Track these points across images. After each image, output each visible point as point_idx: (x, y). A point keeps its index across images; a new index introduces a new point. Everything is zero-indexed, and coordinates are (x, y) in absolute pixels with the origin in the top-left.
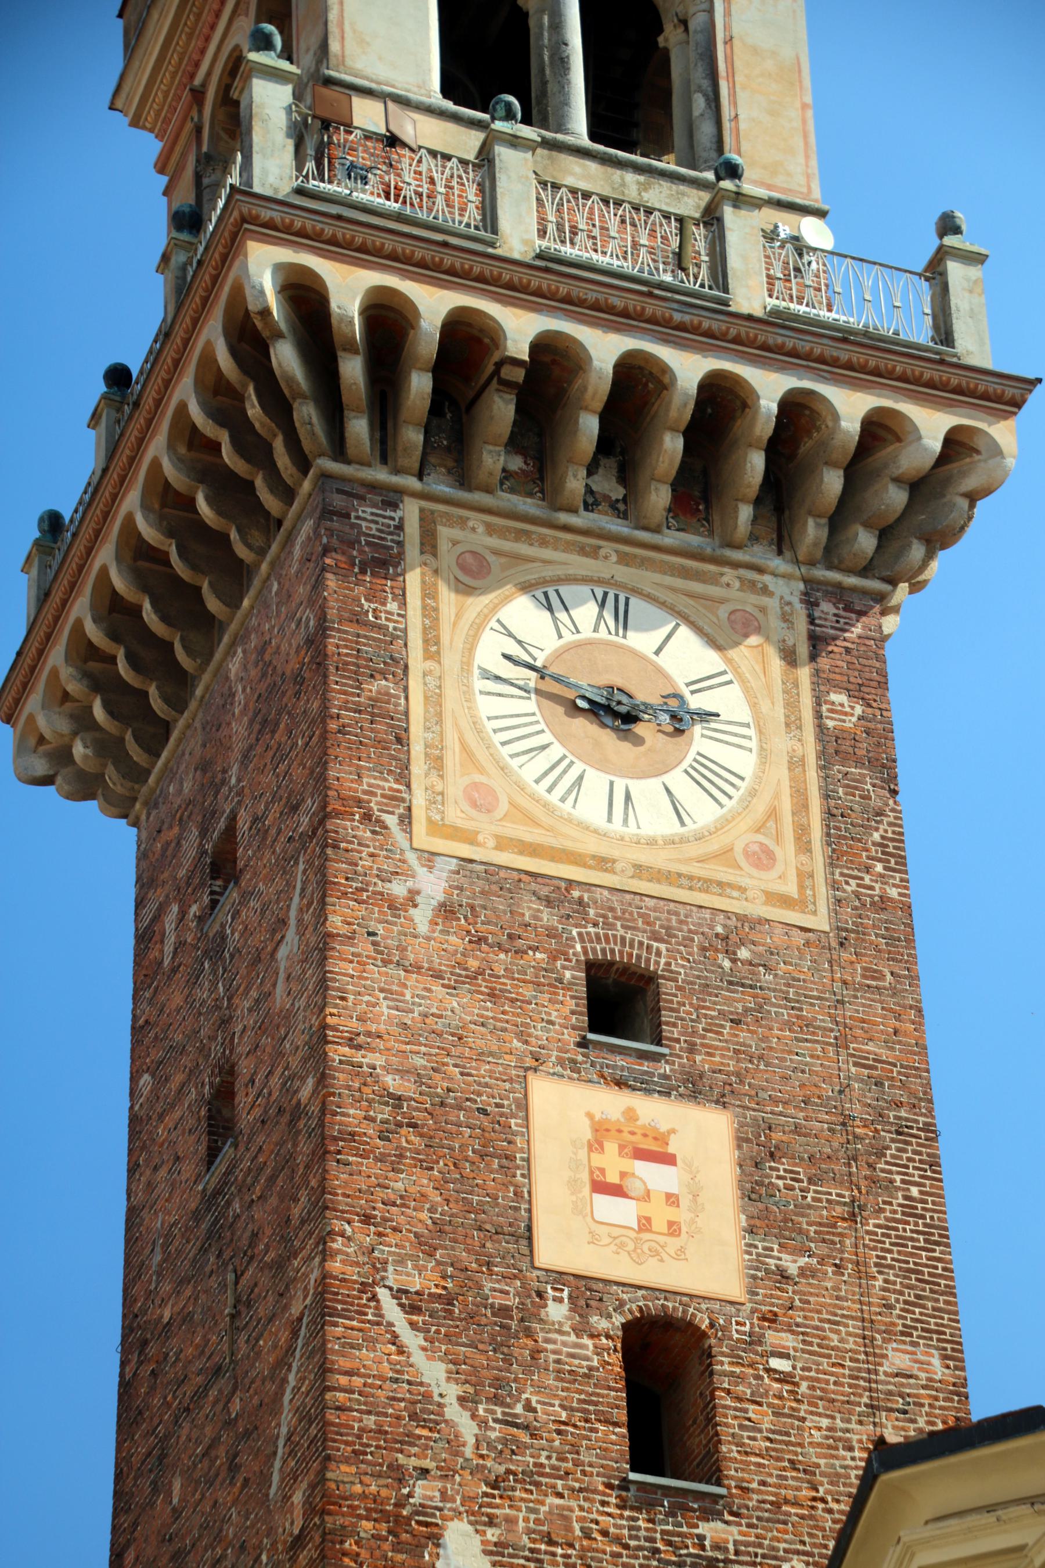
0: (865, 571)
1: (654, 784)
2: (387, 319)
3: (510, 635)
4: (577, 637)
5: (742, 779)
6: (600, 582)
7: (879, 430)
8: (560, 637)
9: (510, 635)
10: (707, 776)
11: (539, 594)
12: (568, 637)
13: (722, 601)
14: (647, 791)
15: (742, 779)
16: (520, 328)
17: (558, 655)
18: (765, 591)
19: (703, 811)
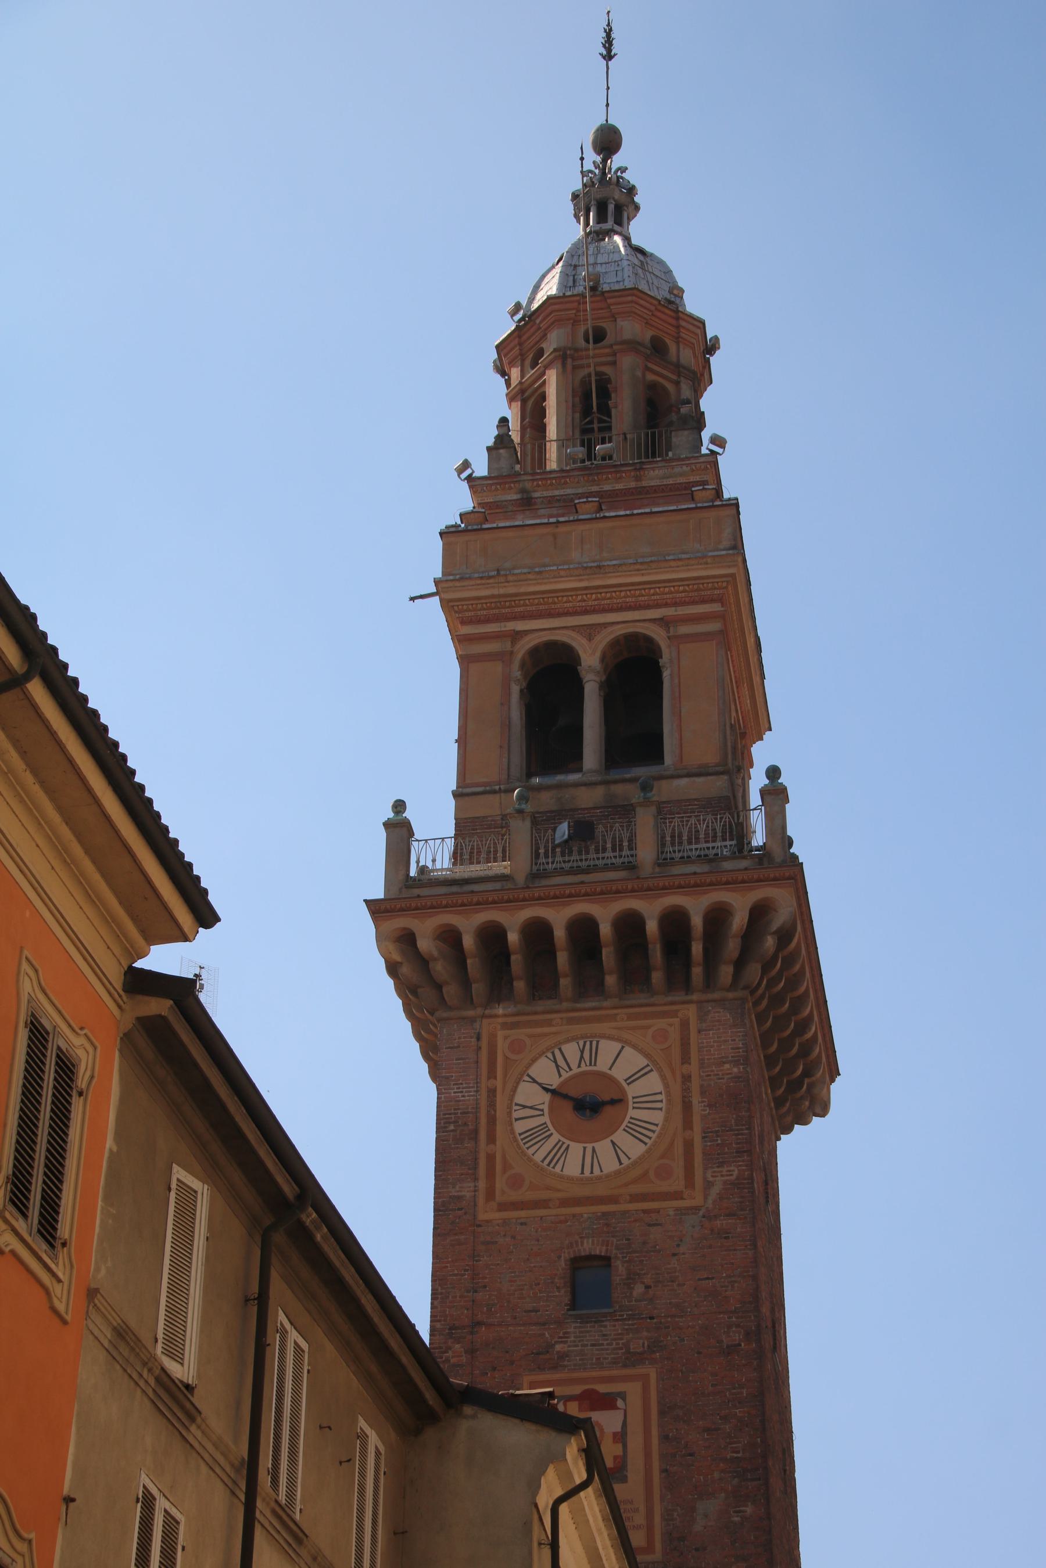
0: (728, 990)
1: (607, 1143)
2: (451, 937)
3: (534, 1081)
4: (570, 1073)
5: (657, 1125)
6: (582, 1038)
7: (717, 918)
8: (560, 1076)
9: (534, 1081)
10: (636, 1130)
11: (550, 1055)
12: (565, 1075)
13: (648, 1027)
14: (603, 1147)
15: (657, 1125)
16: (514, 923)
17: (563, 1084)
18: (674, 1014)
19: (635, 1149)
